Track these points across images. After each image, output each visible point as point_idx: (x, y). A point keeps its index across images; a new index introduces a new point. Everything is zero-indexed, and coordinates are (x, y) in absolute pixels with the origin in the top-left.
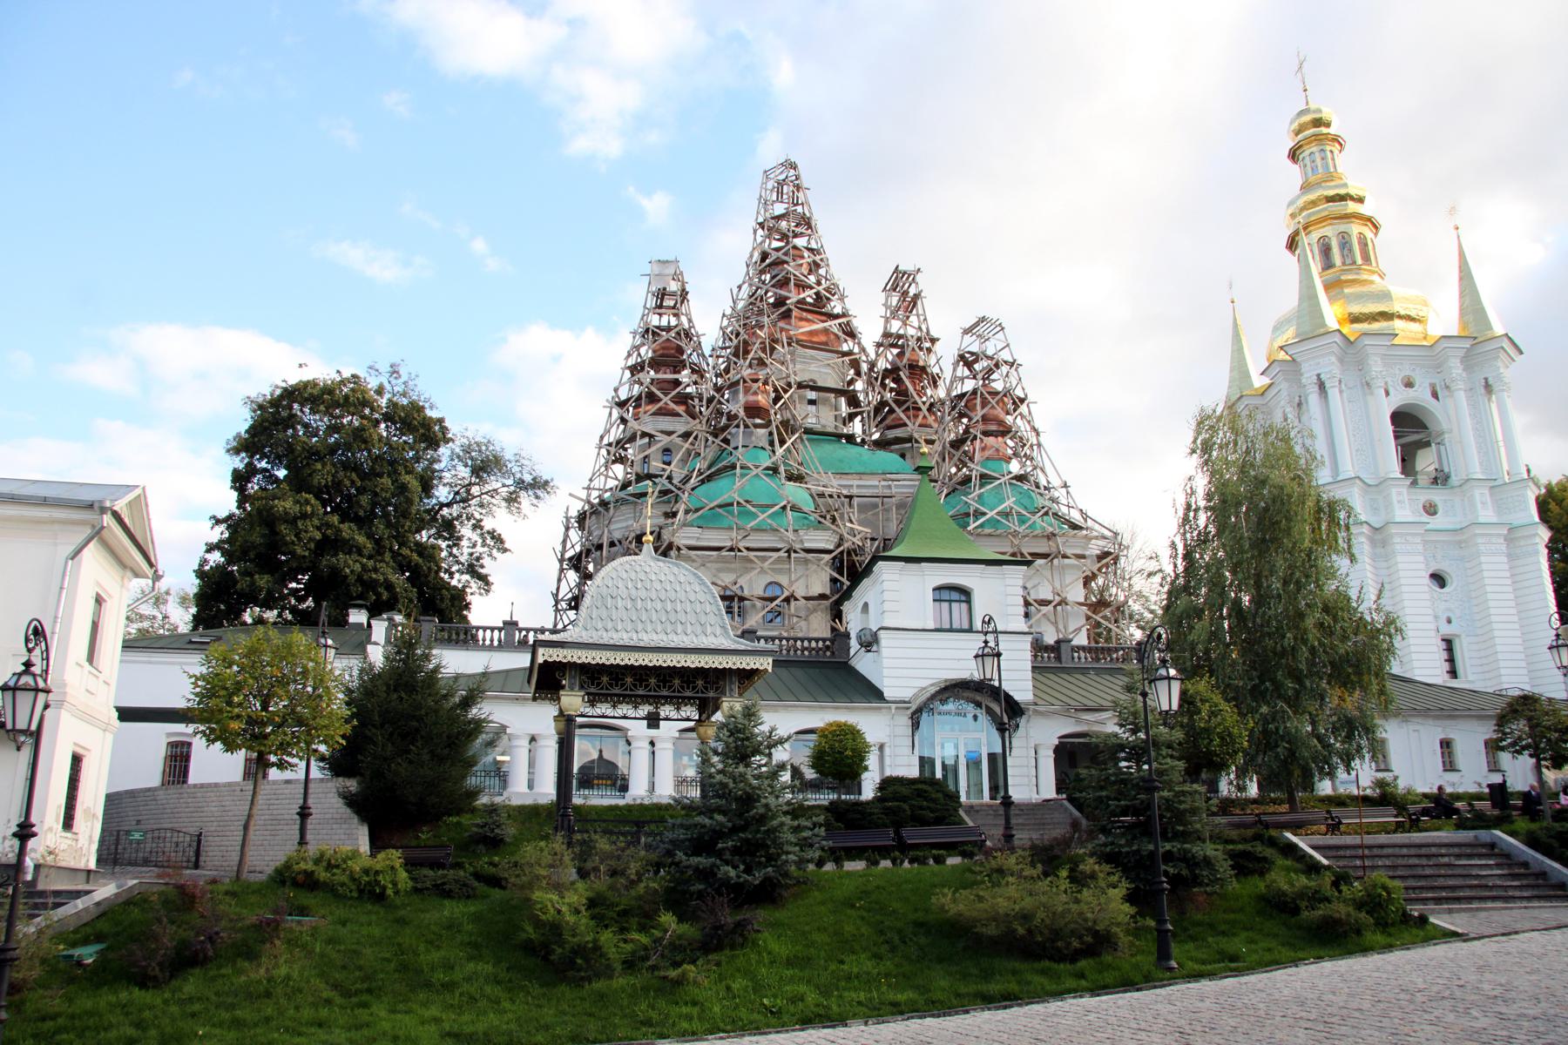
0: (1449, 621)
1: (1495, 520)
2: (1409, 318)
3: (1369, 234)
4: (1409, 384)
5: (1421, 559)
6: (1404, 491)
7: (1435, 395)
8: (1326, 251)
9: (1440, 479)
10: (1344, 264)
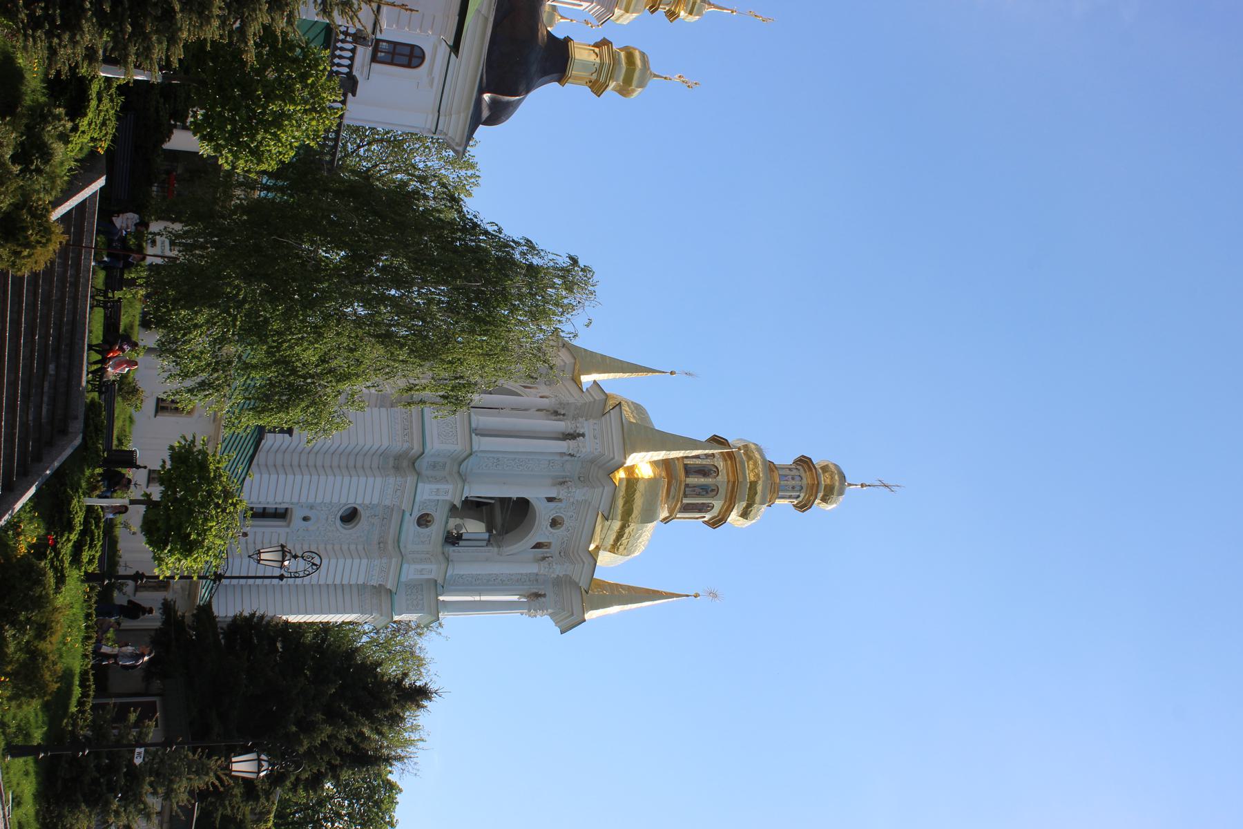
0: (305, 519)
1: (403, 579)
2: (620, 535)
3: (708, 517)
4: (555, 523)
5: (375, 502)
6: (448, 498)
7: (538, 546)
8: (703, 471)
9: (453, 539)
10: (687, 486)
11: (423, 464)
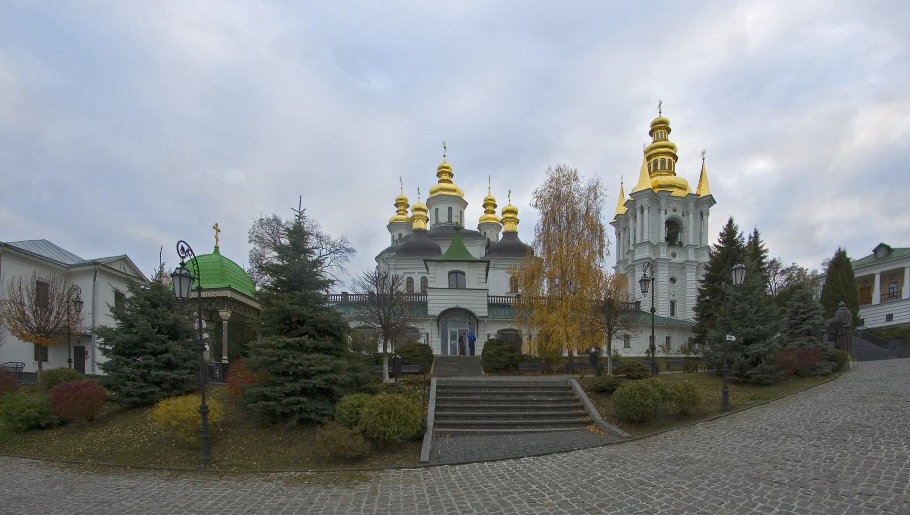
4: (675, 210)
8: (656, 164)
11: (654, 258)
